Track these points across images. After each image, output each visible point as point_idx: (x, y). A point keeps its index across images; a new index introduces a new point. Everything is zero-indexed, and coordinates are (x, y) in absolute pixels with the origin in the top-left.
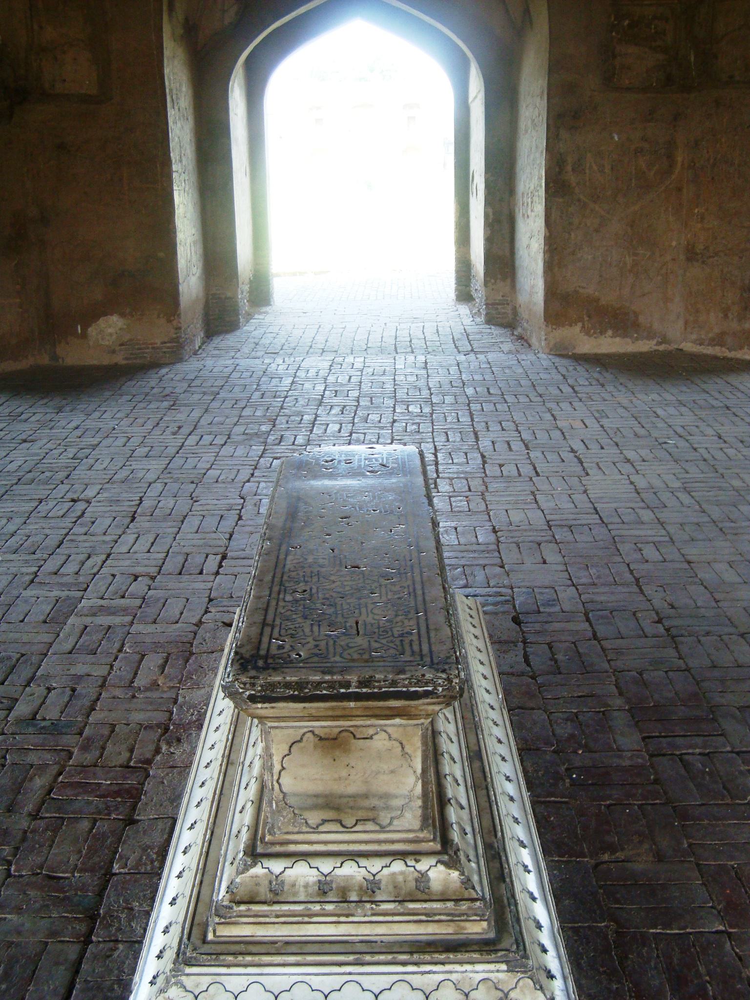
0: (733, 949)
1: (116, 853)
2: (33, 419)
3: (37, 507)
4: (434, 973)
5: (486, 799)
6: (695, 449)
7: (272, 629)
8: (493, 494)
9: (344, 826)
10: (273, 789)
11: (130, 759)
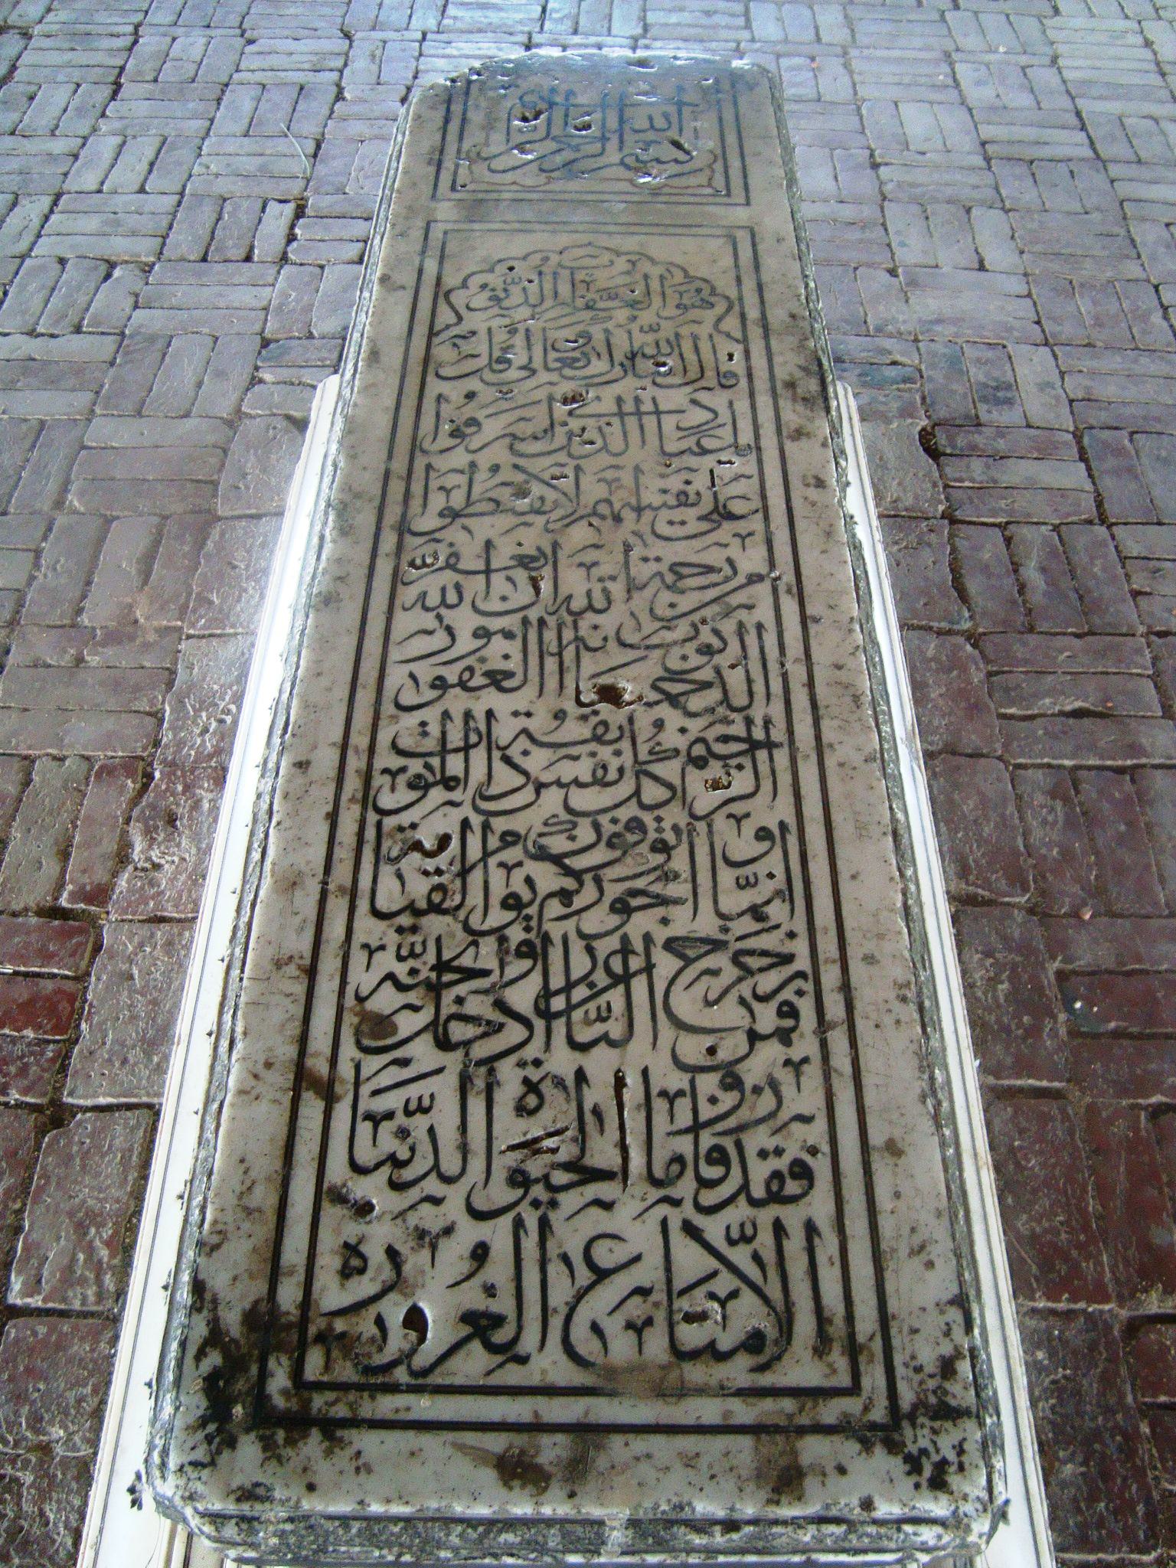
8: (866, 52)
11: (60, 886)
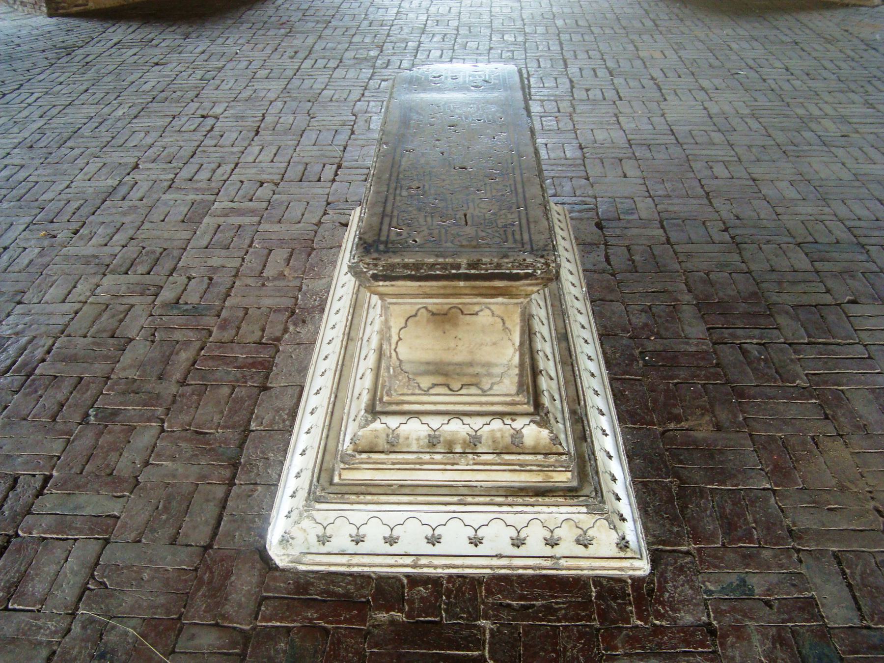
0: (777, 503)
1: (252, 413)
2: (163, 44)
3: (170, 123)
4: (525, 513)
5: (571, 373)
6: (764, 80)
7: (391, 219)
9: (451, 390)
10: (391, 357)
11: (262, 337)
